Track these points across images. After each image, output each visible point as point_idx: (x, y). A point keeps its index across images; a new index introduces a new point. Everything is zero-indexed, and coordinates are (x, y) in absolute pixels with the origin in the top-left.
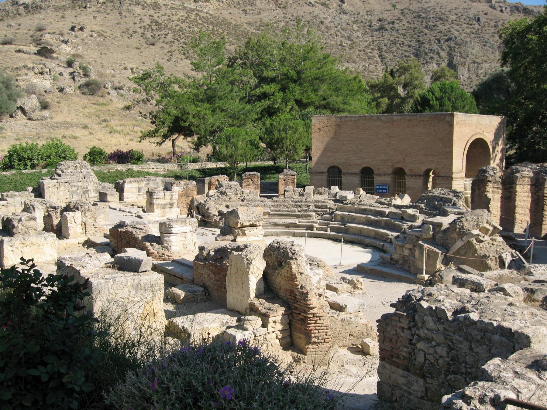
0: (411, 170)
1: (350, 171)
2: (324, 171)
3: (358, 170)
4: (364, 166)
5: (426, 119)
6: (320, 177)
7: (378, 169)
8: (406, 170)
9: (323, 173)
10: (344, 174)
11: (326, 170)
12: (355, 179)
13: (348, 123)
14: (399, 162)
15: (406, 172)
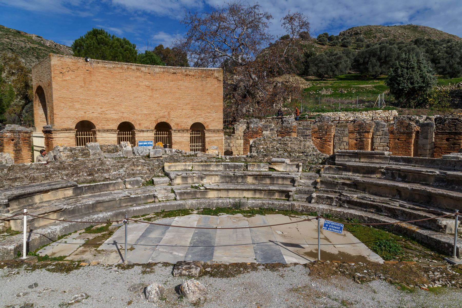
0: (177, 124)
1: (106, 127)
2: (71, 127)
3: (115, 126)
4: (123, 121)
5: (191, 73)
6: (67, 135)
7: (140, 124)
8: (172, 125)
9: (71, 130)
10: (99, 131)
11: (74, 126)
12: (113, 135)
13: (101, 71)
14: (164, 117)
15: (172, 126)
